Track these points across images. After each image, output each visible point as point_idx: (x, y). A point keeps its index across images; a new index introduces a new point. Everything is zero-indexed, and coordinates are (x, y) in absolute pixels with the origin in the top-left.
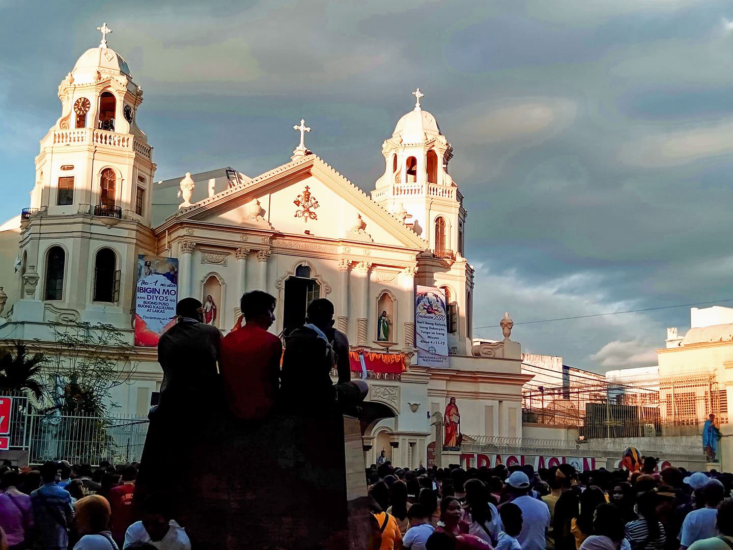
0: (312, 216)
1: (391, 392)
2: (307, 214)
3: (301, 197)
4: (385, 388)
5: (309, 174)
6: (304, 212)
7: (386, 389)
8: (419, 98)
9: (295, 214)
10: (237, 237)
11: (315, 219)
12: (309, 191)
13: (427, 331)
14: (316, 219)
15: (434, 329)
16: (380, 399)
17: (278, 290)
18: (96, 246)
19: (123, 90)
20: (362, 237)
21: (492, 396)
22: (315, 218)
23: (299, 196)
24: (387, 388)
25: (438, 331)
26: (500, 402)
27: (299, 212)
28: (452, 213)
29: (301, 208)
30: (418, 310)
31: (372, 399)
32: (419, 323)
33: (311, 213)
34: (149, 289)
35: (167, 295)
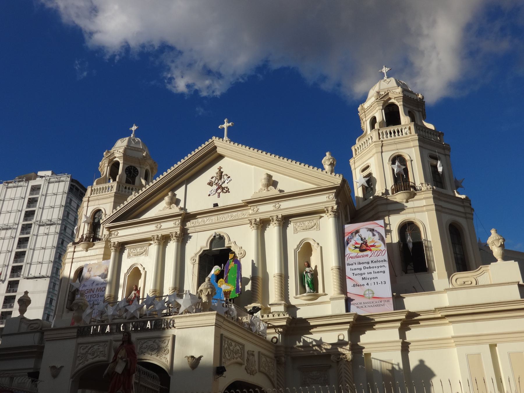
2: (219, 191)
3: (214, 179)
4: (153, 340)
5: (220, 157)
6: (217, 190)
8: (386, 72)
12: (222, 170)
13: (360, 272)
14: (229, 192)
15: (370, 268)
19: (120, 156)
20: (273, 192)
22: (228, 191)
23: (212, 178)
25: (376, 270)
26: (493, 347)
27: (213, 191)
28: (411, 147)
30: (347, 251)
32: (349, 264)
33: (223, 189)
34: (87, 291)
35: (99, 292)
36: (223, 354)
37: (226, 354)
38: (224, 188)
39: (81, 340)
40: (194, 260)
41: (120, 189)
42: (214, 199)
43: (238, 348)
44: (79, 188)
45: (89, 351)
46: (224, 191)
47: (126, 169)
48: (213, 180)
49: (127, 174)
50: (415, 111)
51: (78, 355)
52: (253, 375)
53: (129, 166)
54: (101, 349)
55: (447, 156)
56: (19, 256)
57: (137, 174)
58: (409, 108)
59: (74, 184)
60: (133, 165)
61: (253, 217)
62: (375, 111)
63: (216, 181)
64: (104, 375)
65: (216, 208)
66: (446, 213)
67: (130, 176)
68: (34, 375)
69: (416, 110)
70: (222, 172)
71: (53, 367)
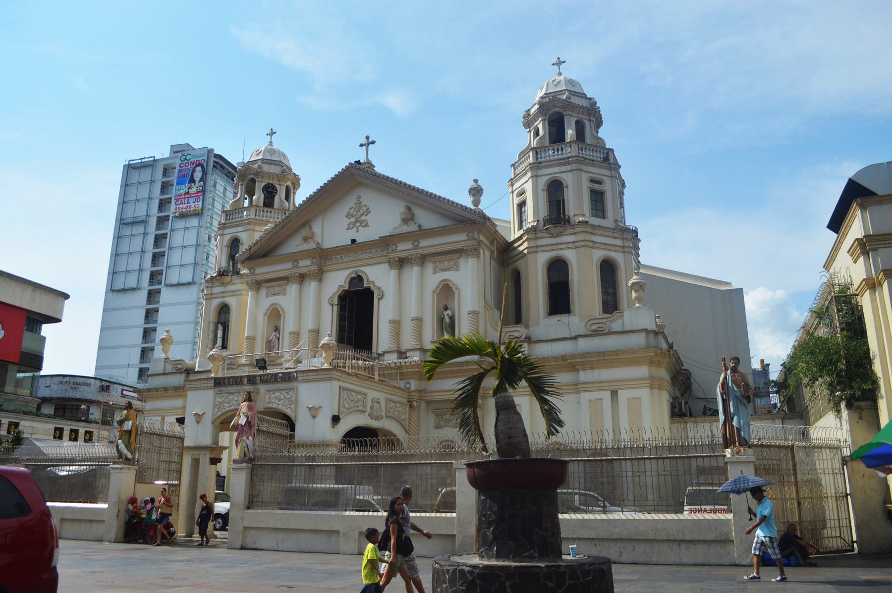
0: (364, 225)
1: (288, 396)
2: (358, 224)
3: (353, 209)
7: (281, 393)
9: (347, 227)
10: (289, 265)
11: (366, 227)
16: (274, 405)
17: (331, 307)
18: (216, 303)
20: (413, 228)
21: (598, 386)
22: (367, 225)
23: (350, 209)
24: (283, 392)
26: (614, 394)
29: (353, 219)
31: (267, 406)
33: (362, 222)
36: (342, 404)
37: (345, 403)
38: (363, 220)
39: (217, 389)
40: (332, 301)
41: (257, 214)
42: (352, 234)
43: (359, 397)
44: (224, 165)
45: (226, 401)
46: (364, 225)
47: (264, 188)
48: (352, 211)
49: (264, 194)
50: (584, 120)
51: (217, 403)
52: (378, 420)
53: (265, 184)
54: (236, 398)
55: (613, 178)
56: (156, 258)
57: (276, 193)
58: (578, 117)
59: (218, 160)
60: (270, 182)
61: (391, 255)
62: (538, 122)
63: (355, 213)
64: (231, 426)
65: (354, 245)
66: (599, 248)
67: (268, 196)
68: (181, 421)
69: (586, 120)
70: (360, 203)
71: (196, 414)
